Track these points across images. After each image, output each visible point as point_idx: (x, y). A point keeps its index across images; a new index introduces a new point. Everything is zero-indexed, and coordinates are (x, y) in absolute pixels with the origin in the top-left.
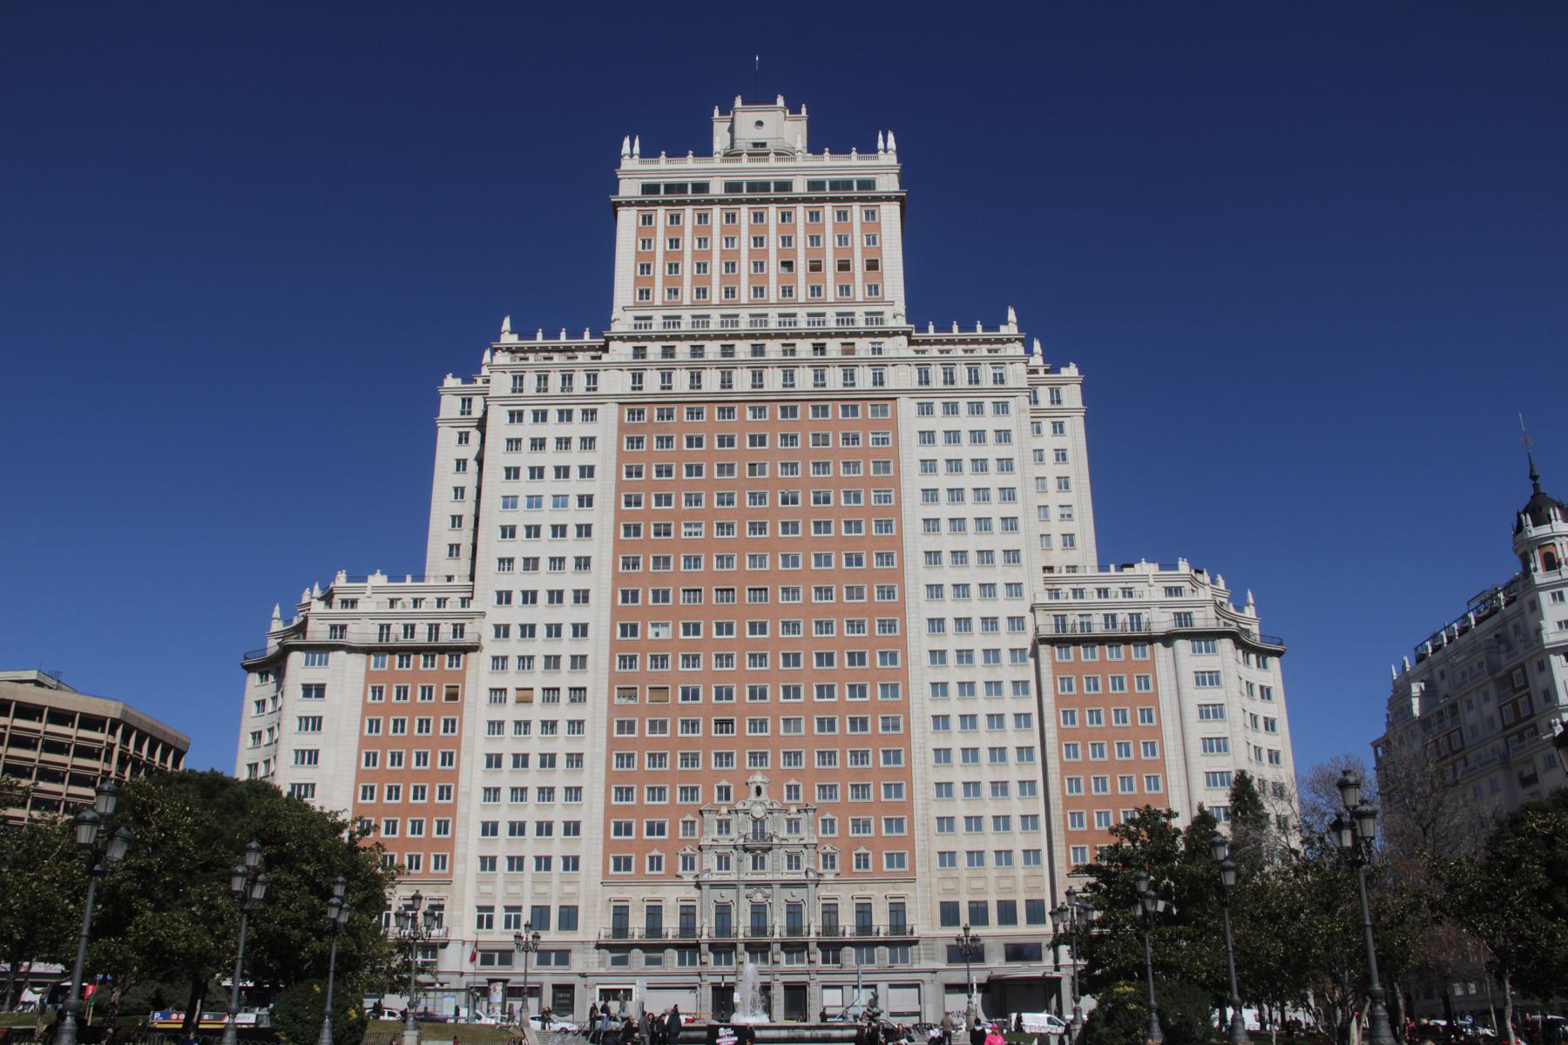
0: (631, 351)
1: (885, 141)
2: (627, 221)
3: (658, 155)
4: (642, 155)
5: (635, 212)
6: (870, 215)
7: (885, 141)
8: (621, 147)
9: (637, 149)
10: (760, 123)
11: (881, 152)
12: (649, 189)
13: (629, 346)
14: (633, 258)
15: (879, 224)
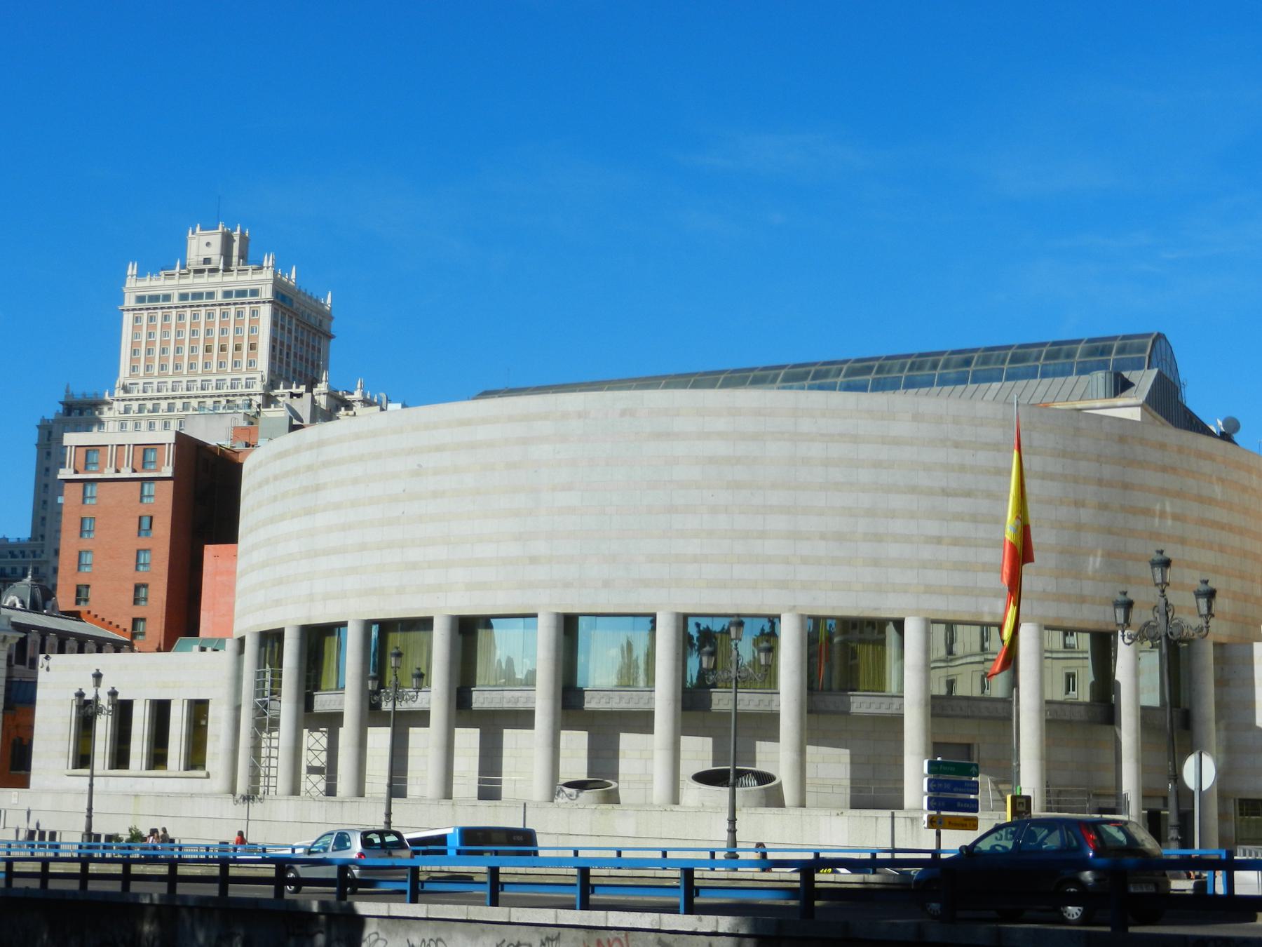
0: (122, 409)
1: (268, 260)
2: (128, 318)
3: (145, 275)
4: (137, 276)
5: (132, 315)
6: (254, 313)
7: (268, 260)
8: (127, 269)
9: (135, 272)
10: (208, 244)
11: (265, 269)
12: (140, 299)
13: (123, 404)
14: (129, 345)
15: (259, 319)
